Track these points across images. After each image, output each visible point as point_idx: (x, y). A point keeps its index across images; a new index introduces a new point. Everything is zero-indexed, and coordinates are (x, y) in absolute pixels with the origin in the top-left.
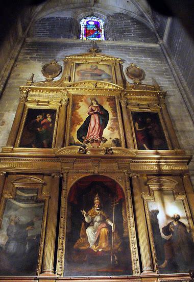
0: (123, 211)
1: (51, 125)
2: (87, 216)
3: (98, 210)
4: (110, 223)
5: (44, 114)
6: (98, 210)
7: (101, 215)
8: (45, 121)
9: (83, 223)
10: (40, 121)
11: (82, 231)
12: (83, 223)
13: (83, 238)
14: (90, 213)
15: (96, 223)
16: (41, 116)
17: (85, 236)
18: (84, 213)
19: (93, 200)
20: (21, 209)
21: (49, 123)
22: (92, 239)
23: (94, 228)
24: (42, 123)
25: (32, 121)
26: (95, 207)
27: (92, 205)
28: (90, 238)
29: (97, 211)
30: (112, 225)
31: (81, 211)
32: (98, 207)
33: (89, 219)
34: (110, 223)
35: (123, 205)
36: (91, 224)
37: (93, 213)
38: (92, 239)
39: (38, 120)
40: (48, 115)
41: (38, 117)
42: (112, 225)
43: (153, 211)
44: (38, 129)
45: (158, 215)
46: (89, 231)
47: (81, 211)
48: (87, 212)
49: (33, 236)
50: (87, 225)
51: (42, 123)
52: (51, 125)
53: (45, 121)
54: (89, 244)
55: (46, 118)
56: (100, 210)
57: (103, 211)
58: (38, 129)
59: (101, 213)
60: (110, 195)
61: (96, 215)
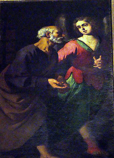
1: (97, 62)
5: (63, 20)
8: (70, 47)
10: (54, 48)
16: (53, 31)
21: (89, 54)
24: (62, 54)
25: (23, 53)
39: (43, 45)
40: (80, 23)
41: (41, 32)
44: (51, 81)
51: (62, 54)
52: (97, 62)
53: (70, 47)
55: (75, 34)
58: (51, 81)
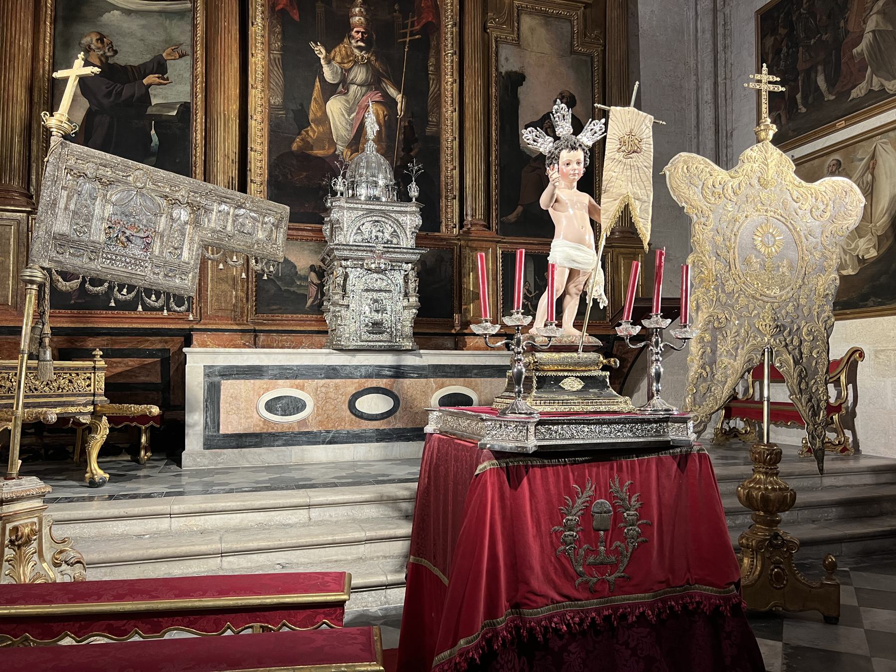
0: (432, 61)
2: (329, 62)
3: (360, 48)
4: (392, 91)
6: (359, 48)
7: (368, 64)
9: (318, 84)
11: (313, 106)
12: (318, 84)
13: (317, 125)
14: (339, 52)
15: (353, 88)
17: (324, 119)
18: (320, 51)
19: (348, 17)
20: (116, 12)
22: (343, 133)
23: (347, 101)
26: (351, 37)
27: (348, 28)
28: (336, 129)
29: (357, 52)
30: (399, 98)
31: (312, 45)
32: (362, 40)
33: (334, 73)
34: (392, 91)
35: (433, 43)
36: (340, 88)
37: (348, 56)
38: (343, 133)
42: (399, 98)
43: (509, 74)
45: (520, 89)
46: (335, 107)
47: (312, 45)
48: (328, 51)
49: (170, 106)
50: (330, 91)
54: (333, 144)
56: (366, 49)
57: (375, 54)
59: (368, 58)
60: (396, 7)
61: (356, 63)
